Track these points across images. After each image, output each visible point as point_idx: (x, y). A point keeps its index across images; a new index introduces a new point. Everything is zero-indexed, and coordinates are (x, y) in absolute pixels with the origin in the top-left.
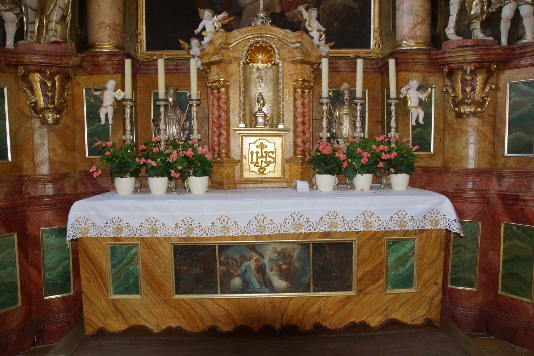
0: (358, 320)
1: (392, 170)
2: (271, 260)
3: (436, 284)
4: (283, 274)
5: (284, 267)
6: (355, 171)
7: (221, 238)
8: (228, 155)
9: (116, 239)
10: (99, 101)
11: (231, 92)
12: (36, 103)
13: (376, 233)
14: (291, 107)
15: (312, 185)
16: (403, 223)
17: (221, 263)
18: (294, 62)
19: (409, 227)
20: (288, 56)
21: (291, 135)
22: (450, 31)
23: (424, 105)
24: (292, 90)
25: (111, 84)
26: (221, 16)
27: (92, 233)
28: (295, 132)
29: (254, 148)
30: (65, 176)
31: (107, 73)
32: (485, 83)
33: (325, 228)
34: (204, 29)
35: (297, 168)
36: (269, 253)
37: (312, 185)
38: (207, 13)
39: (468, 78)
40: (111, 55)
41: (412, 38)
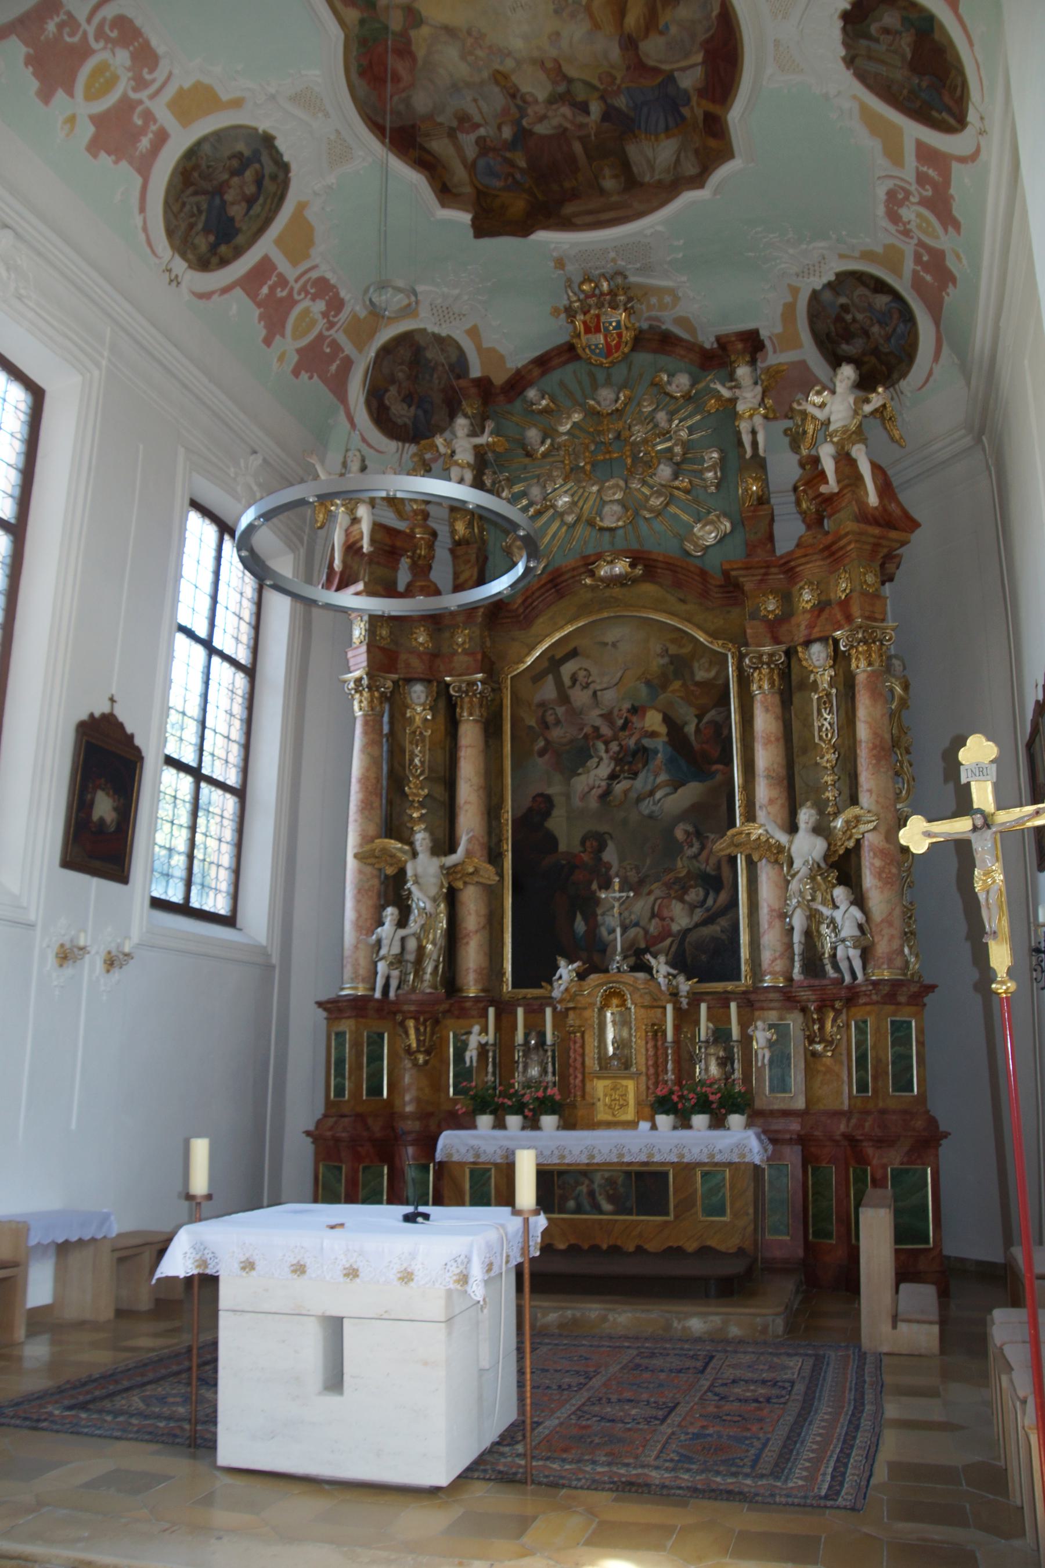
0: (675, 1245)
1: (723, 1111)
2: (600, 1186)
3: (747, 1214)
4: (610, 1199)
5: (611, 1192)
7: (559, 1164)
8: (583, 1097)
9: (474, 1163)
11: (587, 1036)
12: (409, 1046)
13: (688, 1164)
14: (643, 1051)
16: (712, 1156)
17: (559, 1187)
18: (644, 1007)
19: (718, 1158)
20: (639, 1001)
21: (643, 1078)
24: (644, 1034)
25: (476, 1029)
26: (575, 965)
27: (456, 1158)
28: (647, 1075)
30: (431, 1115)
31: (473, 1017)
32: (834, 1020)
33: (643, 1158)
36: (598, 1179)
37: (654, 1127)
38: (562, 963)
39: (815, 1016)
40: (477, 999)
41: (770, 973)
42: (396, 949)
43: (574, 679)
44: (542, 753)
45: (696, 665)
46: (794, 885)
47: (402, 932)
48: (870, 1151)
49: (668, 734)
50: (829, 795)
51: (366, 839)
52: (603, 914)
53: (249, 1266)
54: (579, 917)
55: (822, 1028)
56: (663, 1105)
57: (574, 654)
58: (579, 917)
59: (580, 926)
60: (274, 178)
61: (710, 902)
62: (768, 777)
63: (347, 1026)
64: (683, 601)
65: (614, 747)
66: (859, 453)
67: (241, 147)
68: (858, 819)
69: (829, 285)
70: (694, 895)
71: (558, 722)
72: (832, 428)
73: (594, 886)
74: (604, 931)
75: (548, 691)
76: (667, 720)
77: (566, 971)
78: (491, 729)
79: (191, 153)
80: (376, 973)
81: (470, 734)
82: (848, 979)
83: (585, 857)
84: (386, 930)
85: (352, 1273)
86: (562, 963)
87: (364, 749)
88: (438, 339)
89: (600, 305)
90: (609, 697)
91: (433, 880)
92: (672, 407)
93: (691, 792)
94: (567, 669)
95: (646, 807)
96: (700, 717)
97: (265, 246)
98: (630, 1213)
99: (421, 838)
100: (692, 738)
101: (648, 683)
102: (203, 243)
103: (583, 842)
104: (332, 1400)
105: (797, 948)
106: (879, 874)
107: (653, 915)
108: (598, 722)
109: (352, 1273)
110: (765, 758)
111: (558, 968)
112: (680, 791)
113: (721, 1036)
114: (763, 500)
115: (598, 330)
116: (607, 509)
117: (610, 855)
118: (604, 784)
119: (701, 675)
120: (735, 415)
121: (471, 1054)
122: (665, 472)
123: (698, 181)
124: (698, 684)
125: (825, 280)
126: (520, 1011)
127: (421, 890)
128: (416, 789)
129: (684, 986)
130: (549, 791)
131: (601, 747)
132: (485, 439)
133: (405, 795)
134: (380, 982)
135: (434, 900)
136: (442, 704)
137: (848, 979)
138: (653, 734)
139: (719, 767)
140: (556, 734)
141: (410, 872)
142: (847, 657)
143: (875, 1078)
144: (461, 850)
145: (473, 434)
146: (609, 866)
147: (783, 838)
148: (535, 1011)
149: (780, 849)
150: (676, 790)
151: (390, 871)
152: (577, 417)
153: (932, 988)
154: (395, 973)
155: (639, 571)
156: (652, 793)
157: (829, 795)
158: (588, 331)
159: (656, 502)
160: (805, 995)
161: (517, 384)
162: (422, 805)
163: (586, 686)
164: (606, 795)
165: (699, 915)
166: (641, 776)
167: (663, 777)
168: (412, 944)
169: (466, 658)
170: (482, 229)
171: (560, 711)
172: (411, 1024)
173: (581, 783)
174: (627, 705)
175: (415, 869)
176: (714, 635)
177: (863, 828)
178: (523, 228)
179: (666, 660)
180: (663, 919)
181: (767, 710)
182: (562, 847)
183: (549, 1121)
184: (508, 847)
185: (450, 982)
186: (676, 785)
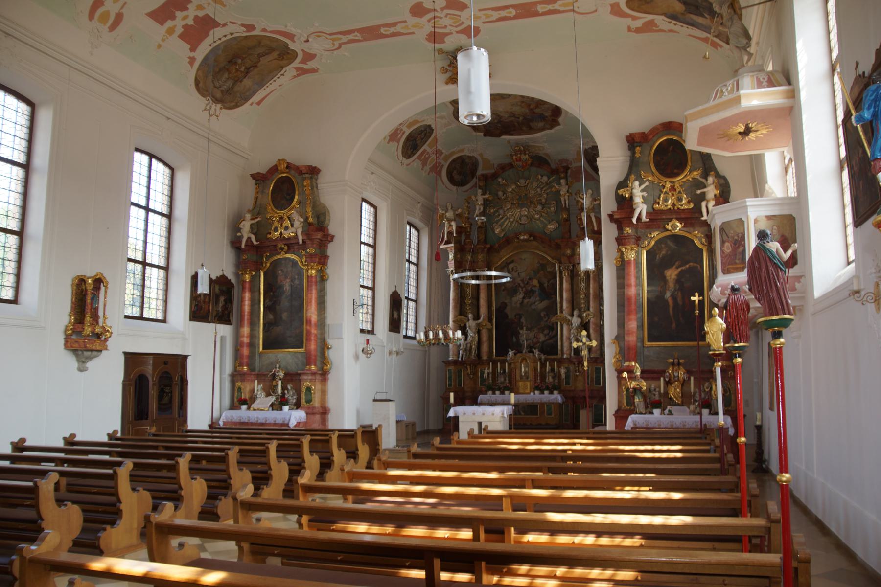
10: (484, 373)
15: (534, 394)
25: (487, 368)
33: (532, 401)
37: (534, 394)
38: (510, 351)
40: (486, 360)
42: (465, 347)
43: (513, 269)
44: (504, 290)
46: (572, 331)
47: (466, 342)
49: (540, 286)
50: (583, 306)
51: (455, 316)
53: (465, 414)
55: (578, 369)
57: (513, 262)
59: (514, 339)
60: (429, 133)
61: (550, 333)
62: (567, 301)
63: (452, 368)
64: (544, 247)
65: (524, 289)
67: (423, 129)
68: (589, 314)
69: (590, 148)
70: (546, 332)
74: (521, 341)
76: (539, 282)
77: (511, 353)
79: (410, 133)
80: (459, 353)
85: (483, 414)
86: (510, 351)
87: (455, 290)
88: (469, 157)
89: (521, 154)
90: (523, 275)
92: (542, 187)
95: (533, 307)
96: (548, 282)
97: (425, 147)
98: (528, 415)
99: (470, 316)
100: (546, 287)
101: (534, 271)
102: (409, 152)
103: (515, 316)
106: (594, 329)
107: (535, 337)
108: (520, 282)
109: (483, 414)
111: (508, 352)
113: (552, 370)
114: (567, 220)
115: (520, 160)
117: (523, 320)
119: (549, 270)
120: (560, 195)
121: (485, 375)
122: (539, 208)
123: (551, 128)
124: (548, 272)
125: (589, 147)
126: (499, 364)
127: (471, 331)
128: (468, 301)
129: (543, 357)
130: (506, 301)
131: (521, 289)
132: (487, 196)
133: (465, 303)
134: (460, 355)
135: (475, 333)
138: (535, 286)
139: (553, 296)
141: (467, 326)
143: (591, 381)
144: (481, 319)
145: (482, 195)
146: (522, 323)
147: (569, 318)
148: (503, 362)
149: (569, 321)
151: (462, 325)
152: (514, 187)
154: (465, 354)
155: (532, 238)
156: (535, 303)
157: (583, 306)
158: (517, 161)
159: (537, 216)
160: (574, 360)
161: (495, 176)
162: (470, 305)
163: (516, 271)
164: (522, 302)
165: (547, 337)
166: (532, 298)
167: (538, 299)
168: (469, 345)
170: (485, 135)
172: (468, 367)
173: (515, 299)
174: (528, 277)
176: (553, 258)
177: (590, 317)
178: (499, 136)
180: (537, 338)
181: (567, 282)
182: (509, 317)
184: (494, 317)
185: (479, 355)
186: (541, 301)
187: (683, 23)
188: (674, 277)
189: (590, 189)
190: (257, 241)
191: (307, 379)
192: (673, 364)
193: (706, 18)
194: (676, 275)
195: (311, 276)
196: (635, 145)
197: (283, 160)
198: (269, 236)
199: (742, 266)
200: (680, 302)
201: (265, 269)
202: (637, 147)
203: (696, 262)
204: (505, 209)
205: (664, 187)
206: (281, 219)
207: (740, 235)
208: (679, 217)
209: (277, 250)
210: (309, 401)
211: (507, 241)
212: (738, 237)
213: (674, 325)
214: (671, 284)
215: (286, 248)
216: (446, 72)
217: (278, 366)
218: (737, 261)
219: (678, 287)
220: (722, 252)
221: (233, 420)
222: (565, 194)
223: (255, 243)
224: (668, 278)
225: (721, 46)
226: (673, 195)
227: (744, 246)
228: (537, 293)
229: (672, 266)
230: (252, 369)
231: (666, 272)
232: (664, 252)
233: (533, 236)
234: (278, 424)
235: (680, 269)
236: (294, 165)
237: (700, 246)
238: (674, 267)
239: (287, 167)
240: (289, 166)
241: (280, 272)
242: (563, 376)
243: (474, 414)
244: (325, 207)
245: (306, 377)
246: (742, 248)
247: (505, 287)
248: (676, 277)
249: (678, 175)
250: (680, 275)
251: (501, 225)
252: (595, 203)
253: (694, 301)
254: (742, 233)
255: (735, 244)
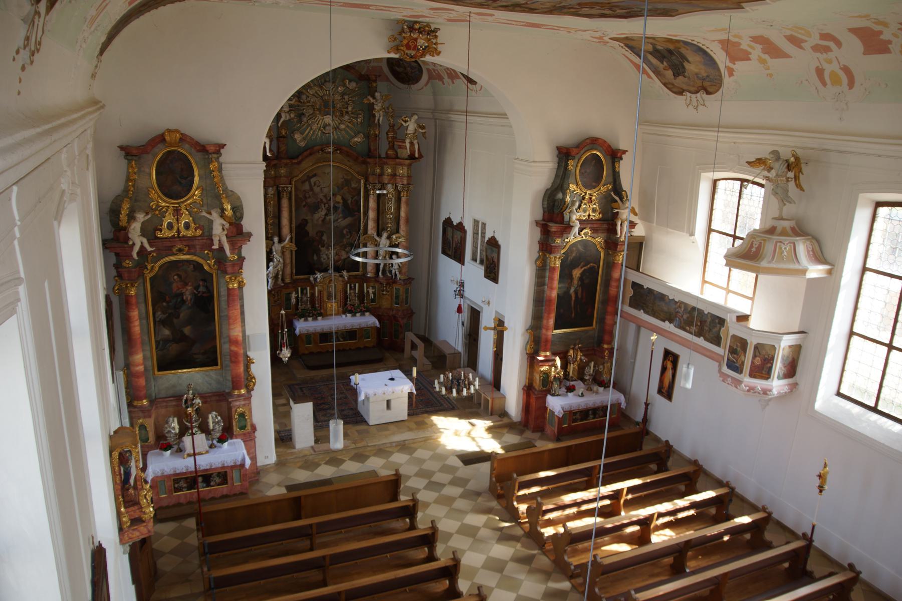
4: (342, 338)
6: (356, 313)
15: (346, 316)
22: (380, 274)
23: (374, 293)
27: (302, 332)
29: (329, 306)
32: (389, 287)
33: (351, 328)
34: (317, 277)
35: (341, 309)
37: (346, 316)
41: (371, 273)
43: (315, 184)
44: (304, 206)
45: (352, 183)
48: (400, 320)
49: (343, 203)
52: (322, 254)
53: (375, 395)
54: (315, 255)
56: (350, 312)
57: (315, 175)
58: (315, 255)
59: (315, 258)
64: (349, 161)
66: (415, 142)
68: (399, 238)
71: (310, 197)
72: (408, 132)
73: (320, 246)
74: (322, 259)
75: (306, 186)
76: (343, 198)
78: (290, 199)
81: (285, 203)
82: (394, 277)
83: (317, 238)
84: (271, 268)
91: (280, 251)
93: (349, 220)
94: (313, 180)
96: (352, 198)
98: (347, 341)
100: (350, 204)
101: (338, 187)
103: (317, 234)
104: (389, 411)
105: (381, 269)
108: (322, 198)
109: (393, 392)
110: (372, 215)
112: (346, 219)
116: (327, 128)
118: (323, 217)
119: (353, 186)
120: (374, 109)
121: (293, 301)
127: (278, 255)
130: (307, 218)
131: (323, 206)
136: (276, 193)
137: (394, 277)
138: (339, 203)
139: (357, 213)
140: (309, 200)
141: (274, 250)
142: (399, 193)
146: (324, 241)
147: (378, 239)
149: (376, 240)
150: (344, 219)
153: (413, 279)
156: (337, 220)
157: (389, 225)
160: (382, 281)
163: (319, 186)
164: (324, 220)
167: (341, 215)
169: (285, 179)
171: (311, 193)
173: (316, 216)
175: (275, 249)
176: (358, 173)
179: (342, 180)
180: (339, 256)
182: (310, 235)
183: (320, 318)
186: (344, 218)
187: (632, 51)
188: (578, 275)
189: (417, 115)
190: (151, 246)
191: (240, 405)
192: (573, 349)
193: (663, 64)
194: (580, 274)
195: (233, 289)
196: (570, 158)
197: (177, 131)
198: (159, 235)
199: (767, 376)
200: (580, 296)
201: (152, 275)
202: (570, 160)
203: (595, 263)
204: (307, 115)
205: (584, 198)
206: (177, 212)
207: (770, 356)
208: (592, 226)
209: (171, 250)
210: (243, 428)
211: (310, 150)
212: (769, 357)
213: (573, 315)
214: (576, 282)
215: (187, 249)
216: (394, 41)
217: (191, 392)
218: (764, 372)
219: (580, 283)
220: (753, 362)
221: (165, 474)
222: (381, 110)
223: (149, 249)
224: (574, 276)
225: (649, 77)
226: (589, 206)
227: (772, 364)
228: (340, 209)
229: (578, 267)
230: (152, 402)
231: (573, 271)
232: (574, 255)
233: (338, 148)
234: (228, 467)
235: (583, 269)
236: (192, 139)
237: (600, 249)
238: (580, 267)
239: (181, 139)
240: (184, 138)
241: (176, 277)
242: (372, 296)
243: (384, 393)
244: (239, 198)
245: (238, 403)
246: (770, 365)
247: (306, 203)
248: (579, 275)
249: (594, 187)
250: (582, 274)
251: (302, 134)
252: (420, 130)
253: (653, 340)
254: (772, 355)
255: (765, 360)
